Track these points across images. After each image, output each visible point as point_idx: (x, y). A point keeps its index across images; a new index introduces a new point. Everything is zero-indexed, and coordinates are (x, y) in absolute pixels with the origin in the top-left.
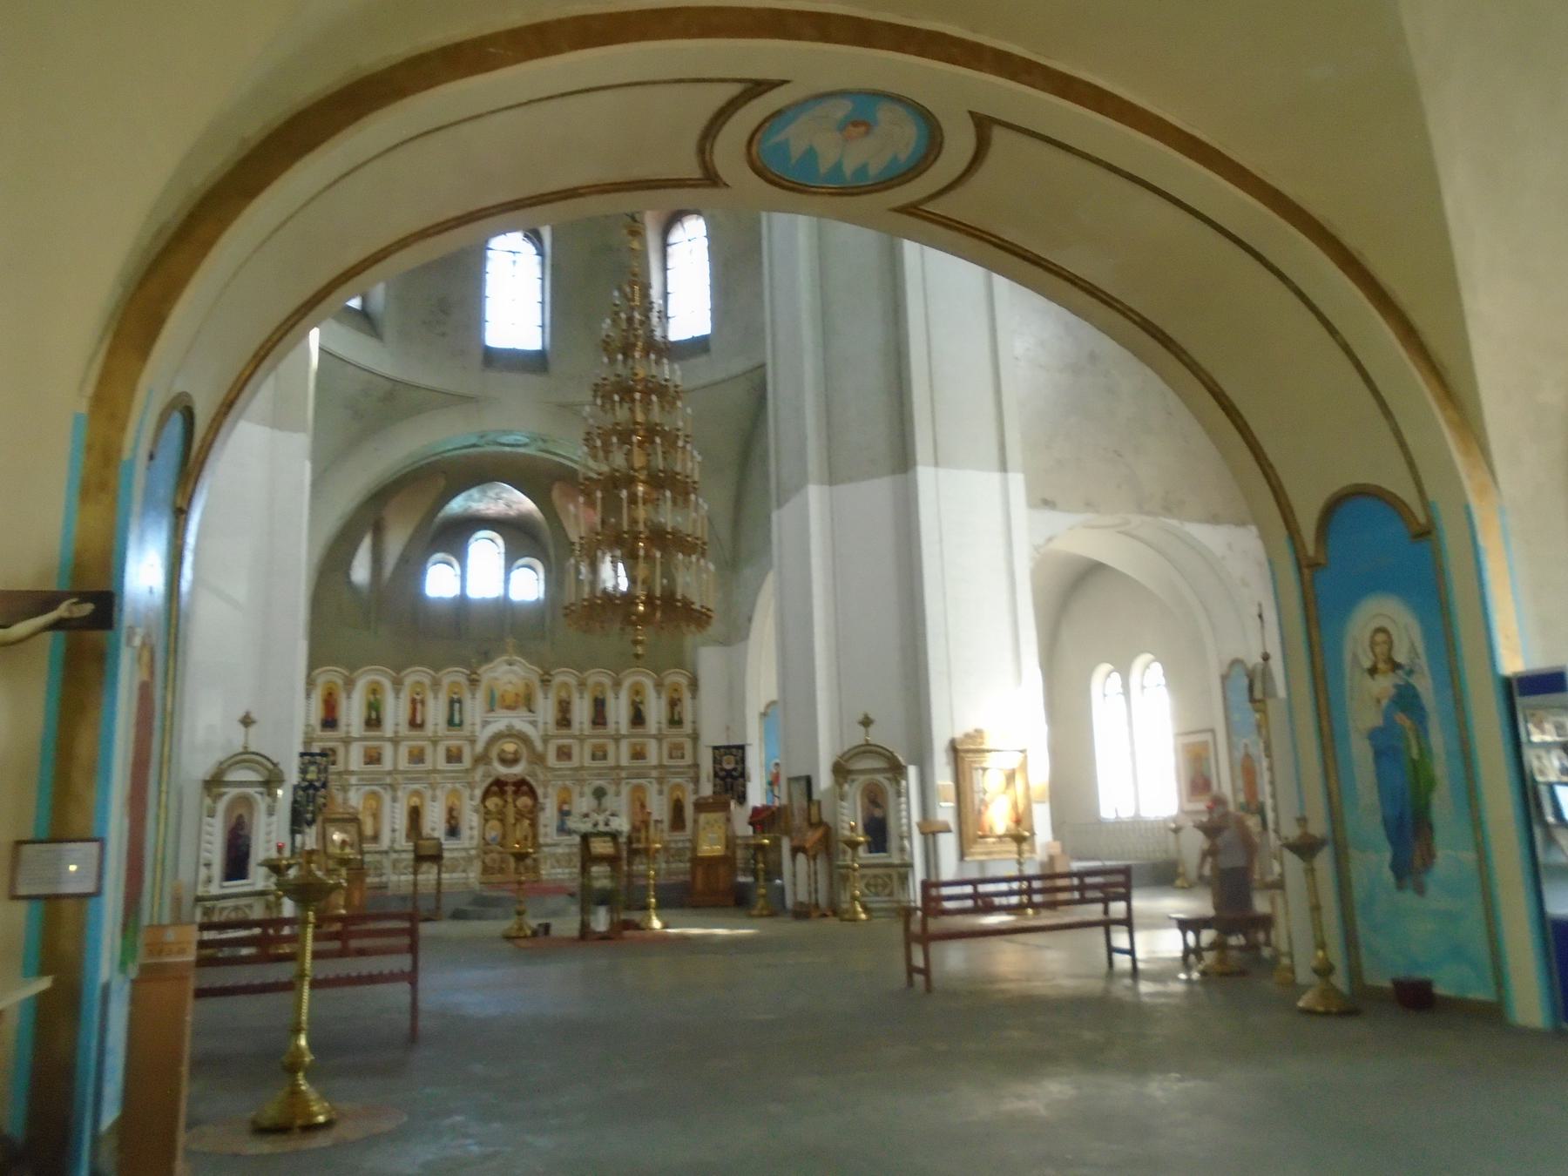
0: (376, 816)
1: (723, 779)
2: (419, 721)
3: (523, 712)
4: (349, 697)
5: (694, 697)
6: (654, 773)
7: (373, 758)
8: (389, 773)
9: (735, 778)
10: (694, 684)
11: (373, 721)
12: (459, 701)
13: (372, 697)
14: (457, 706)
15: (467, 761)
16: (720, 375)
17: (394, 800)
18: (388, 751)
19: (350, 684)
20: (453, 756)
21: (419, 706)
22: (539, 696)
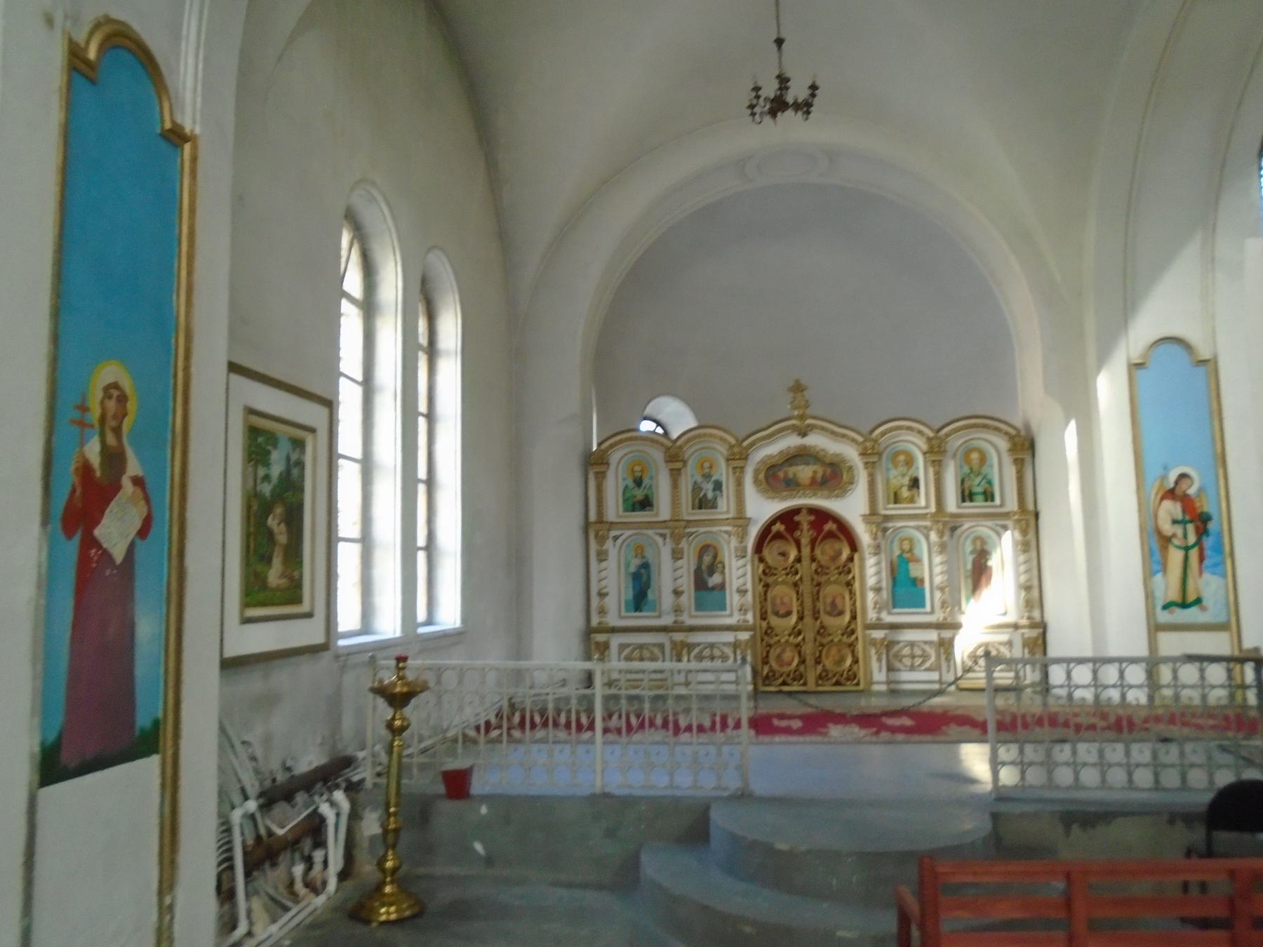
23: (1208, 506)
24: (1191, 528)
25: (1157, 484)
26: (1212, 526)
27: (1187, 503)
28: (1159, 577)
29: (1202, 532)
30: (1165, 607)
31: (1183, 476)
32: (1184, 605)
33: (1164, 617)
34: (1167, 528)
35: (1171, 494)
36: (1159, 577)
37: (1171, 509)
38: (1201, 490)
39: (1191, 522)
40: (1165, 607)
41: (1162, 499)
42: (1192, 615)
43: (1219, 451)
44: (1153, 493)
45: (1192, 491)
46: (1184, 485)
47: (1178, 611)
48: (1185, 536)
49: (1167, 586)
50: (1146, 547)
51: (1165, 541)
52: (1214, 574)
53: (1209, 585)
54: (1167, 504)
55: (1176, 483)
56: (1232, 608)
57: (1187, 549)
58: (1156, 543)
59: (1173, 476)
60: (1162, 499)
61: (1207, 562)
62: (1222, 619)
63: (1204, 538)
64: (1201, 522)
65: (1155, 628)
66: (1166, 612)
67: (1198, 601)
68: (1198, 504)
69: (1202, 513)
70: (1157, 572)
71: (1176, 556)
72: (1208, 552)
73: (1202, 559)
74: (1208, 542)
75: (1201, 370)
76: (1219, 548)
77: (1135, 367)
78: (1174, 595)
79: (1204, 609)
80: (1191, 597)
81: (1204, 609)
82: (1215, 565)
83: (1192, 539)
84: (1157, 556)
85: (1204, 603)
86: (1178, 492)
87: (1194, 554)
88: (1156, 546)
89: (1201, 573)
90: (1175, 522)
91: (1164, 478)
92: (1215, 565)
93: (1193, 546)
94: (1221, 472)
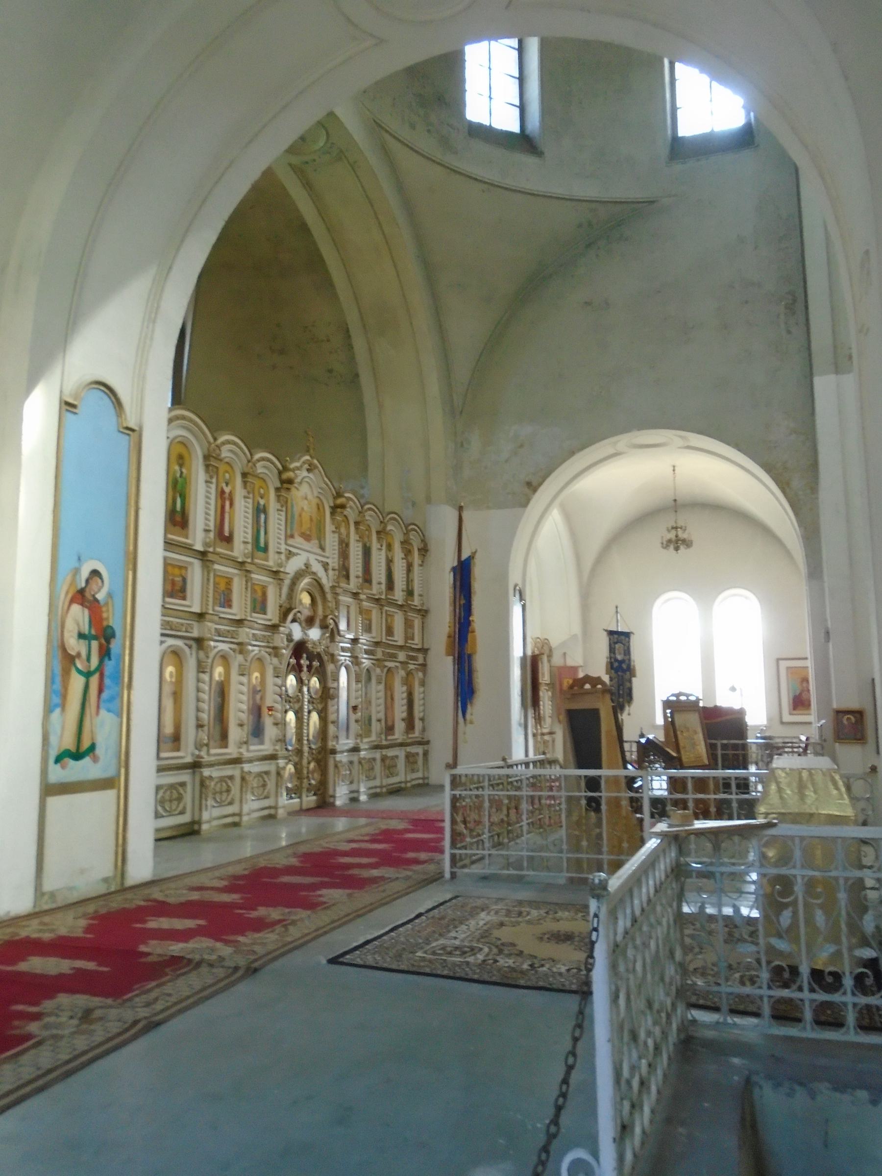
0: (177, 696)
1: (617, 670)
3: (313, 546)
6: (402, 656)
8: (201, 616)
9: (624, 671)
10: (424, 551)
12: (265, 510)
13: (177, 468)
14: (263, 516)
15: (272, 614)
16: (559, 191)
17: (201, 668)
18: (196, 574)
21: (227, 503)
22: (329, 527)
23: (114, 620)
24: (95, 644)
25: (69, 578)
26: (115, 646)
28: (58, 711)
29: (105, 653)
30: (58, 760)
31: (95, 573)
32: (77, 755)
33: (57, 774)
34: (74, 645)
35: (81, 596)
36: (58, 711)
38: (110, 595)
39: (96, 638)
41: (72, 601)
42: (83, 770)
43: (131, 548)
45: (100, 596)
46: (94, 586)
47: (71, 763)
48: (88, 659)
51: (69, 659)
52: (109, 711)
53: (103, 728)
54: (76, 608)
56: (123, 757)
58: (62, 660)
59: (85, 573)
60: (72, 601)
62: (110, 773)
63: (106, 659)
66: (58, 766)
67: (92, 748)
70: (56, 706)
71: (77, 682)
72: (107, 681)
73: (101, 691)
74: (109, 666)
76: (117, 677)
77: (68, 406)
78: (69, 743)
79: (95, 760)
80: (86, 744)
81: (95, 760)
82: (111, 699)
83: (95, 661)
84: (58, 686)
85: (99, 751)
86: (88, 595)
87: (94, 680)
88: (58, 669)
89: (97, 713)
90: (81, 636)
91: (77, 571)
92: (111, 699)
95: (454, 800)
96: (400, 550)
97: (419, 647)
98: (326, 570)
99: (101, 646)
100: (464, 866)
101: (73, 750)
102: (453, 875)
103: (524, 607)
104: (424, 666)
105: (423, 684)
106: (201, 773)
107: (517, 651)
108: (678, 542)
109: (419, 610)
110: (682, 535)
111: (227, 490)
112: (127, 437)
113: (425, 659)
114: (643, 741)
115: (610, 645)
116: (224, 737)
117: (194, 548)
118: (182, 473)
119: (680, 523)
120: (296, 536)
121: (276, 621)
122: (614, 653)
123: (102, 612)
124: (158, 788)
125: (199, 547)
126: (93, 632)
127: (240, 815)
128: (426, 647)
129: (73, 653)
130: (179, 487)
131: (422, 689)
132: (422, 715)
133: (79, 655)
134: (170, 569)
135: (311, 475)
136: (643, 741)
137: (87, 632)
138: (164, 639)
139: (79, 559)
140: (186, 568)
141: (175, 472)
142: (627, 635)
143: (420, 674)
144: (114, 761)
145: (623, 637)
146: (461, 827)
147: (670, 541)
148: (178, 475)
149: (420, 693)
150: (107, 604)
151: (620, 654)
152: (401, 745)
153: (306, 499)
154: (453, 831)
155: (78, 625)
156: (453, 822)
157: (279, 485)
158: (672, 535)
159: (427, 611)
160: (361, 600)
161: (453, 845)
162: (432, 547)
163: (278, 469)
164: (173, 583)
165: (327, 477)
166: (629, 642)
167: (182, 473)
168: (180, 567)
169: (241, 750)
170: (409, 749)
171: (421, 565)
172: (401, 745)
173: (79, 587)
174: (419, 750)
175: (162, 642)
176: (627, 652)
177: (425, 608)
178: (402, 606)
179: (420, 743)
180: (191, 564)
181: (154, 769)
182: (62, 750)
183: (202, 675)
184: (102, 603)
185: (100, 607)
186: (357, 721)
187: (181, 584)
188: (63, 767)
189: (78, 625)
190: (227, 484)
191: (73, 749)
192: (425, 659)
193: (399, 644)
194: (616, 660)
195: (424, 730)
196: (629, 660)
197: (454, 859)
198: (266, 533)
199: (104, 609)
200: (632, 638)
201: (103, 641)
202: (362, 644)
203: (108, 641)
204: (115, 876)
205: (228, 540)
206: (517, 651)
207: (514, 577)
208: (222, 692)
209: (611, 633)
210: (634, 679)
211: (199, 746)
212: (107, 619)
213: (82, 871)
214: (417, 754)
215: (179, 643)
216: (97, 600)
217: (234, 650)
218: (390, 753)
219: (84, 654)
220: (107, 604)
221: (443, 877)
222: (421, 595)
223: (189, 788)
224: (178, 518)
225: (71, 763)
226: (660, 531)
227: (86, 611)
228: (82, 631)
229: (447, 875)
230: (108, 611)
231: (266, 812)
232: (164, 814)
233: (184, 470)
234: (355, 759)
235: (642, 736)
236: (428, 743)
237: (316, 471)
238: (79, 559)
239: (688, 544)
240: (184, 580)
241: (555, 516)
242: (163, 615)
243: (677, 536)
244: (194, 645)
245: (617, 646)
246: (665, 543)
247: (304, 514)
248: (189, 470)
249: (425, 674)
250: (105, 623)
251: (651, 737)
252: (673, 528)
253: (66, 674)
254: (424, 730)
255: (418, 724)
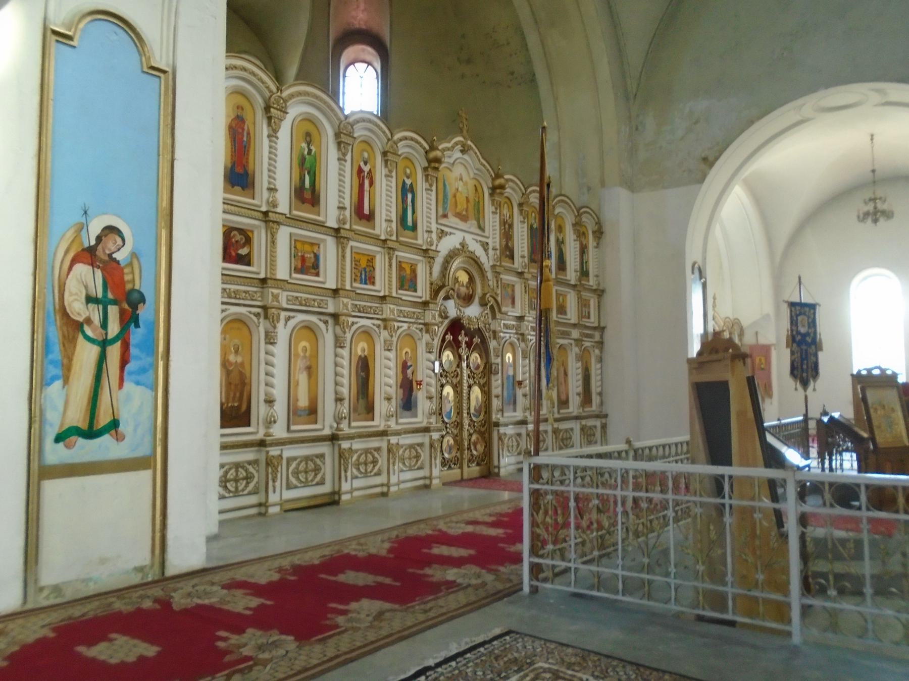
0: (311, 371)
1: (799, 344)
2: (366, 211)
3: (472, 225)
4: (273, 135)
5: (597, 247)
6: (575, 334)
7: (307, 264)
8: (335, 292)
9: (809, 345)
10: (599, 233)
11: (307, 195)
12: (412, 190)
13: (304, 145)
14: (410, 196)
15: (423, 291)
17: (339, 343)
18: (329, 250)
19: (272, 111)
20: (408, 281)
21: (367, 182)
22: (488, 208)
24: (113, 311)
25: (70, 235)
26: (144, 312)
27: (112, 271)
28: (58, 384)
29: (129, 319)
30: (58, 439)
31: (111, 230)
32: (91, 433)
33: (55, 454)
34: (78, 308)
35: (89, 255)
36: (58, 384)
37: (85, 278)
38: (134, 255)
39: (115, 302)
40: (58, 439)
42: (104, 448)
43: (165, 203)
44: (60, 248)
46: (110, 244)
47: (81, 441)
48: (104, 325)
49: (66, 403)
50: (39, 337)
51: (73, 328)
53: (131, 402)
54: (82, 269)
55: (99, 239)
57: (104, 344)
59: (95, 228)
61: (128, 367)
62: (144, 451)
64: (130, 304)
65: (39, 473)
66: (61, 444)
68: (127, 278)
69: (133, 290)
70: (54, 378)
71: (86, 354)
72: (133, 351)
74: (136, 335)
75: (152, 83)
76: (150, 346)
77: (55, 38)
78: (77, 416)
79: (119, 438)
80: (104, 419)
81: (119, 438)
82: (143, 370)
83: (114, 328)
84: (56, 353)
85: (121, 428)
86: (100, 252)
87: (114, 352)
88: (55, 335)
89: (121, 385)
90: (90, 299)
91: (81, 228)
92: (143, 370)
93: (114, 340)
94: (164, 233)
95: (536, 495)
96: (572, 232)
97: (596, 325)
98: (486, 250)
99: (122, 312)
100: (545, 580)
101: (84, 426)
102: (534, 590)
103: (704, 286)
104: (601, 344)
105: (600, 360)
106: (340, 446)
107: (697, 328)
108: (876, 214)
109: (595, 290)
110: (880, 206)
111: (366, 169)
112: (157, 80)
113: (602, 337)
114: (825, 419)
115: (791, 317)
116: (370, 410)
117: (328, 224)
118: (310, 151)
119: (879, 193)
120: (450, 215)
121: (426, 297)
122: (797, 325)
123: (123, 274)
124: (222, 466)
125: (332, 223)
126: (110, 296)
127: (388, 485)
128: (602, 325)
129: (81, 319)
130: (307, 165)
131: (599, 366)
132: (599, 390)
133: (88, 321)
134: (299, 245)
135: (466, 157)
136: (825, 419)
137: (100, 295)
138: (225, 307)
139: (86, 213)
140: (319, 245)
141: (302, 149)
142: (813, 307)
143: (597, 351)
144: (148, 438)
145: (807, 309)
146: (540, 531)
147: (867, 214)
148: (306, 152)
149: (596, 370)
150: (130, 264)
151: (803, 326)
152: (577, 418)
153: (461, 179)
154: (534, 537)
155: (86, 287)
156: (534, 524)
157: (427, 165)
158: (870, 207)
159: (603, 291)
160: (527, 279)
161: (534, 551)
162: (607, 228)
163: (424, 148)
164: (303, 259)
165: (483, 158)
166: (814, 314)
167: (310, 151)
168: (312, 244)
169: (389, 423)
170: (584, 422)
171: (597, 247)
172: (577, 418)
173: (86, 245)
174: (598, 423)
175: (223, 311)
176: (813, 324)
177: (601, 288)
178: (575, 286)
179: (597, 416)
180: (324, 241)
181: (217, 447)
182: (66, 427)
183: (339, 350)
184: (122, 264)
185: (122, 269)
186: (525, 395)
187: (313, 260)
188: (67, 447)
189: (86, 287)
190: (366, 163)
191: (84, 426)
192: (602, 337)
193: (573, 321)
194: (798, 333)
195: (602, 403)
196: (815, 333)
197: (536, 570)
198: (414, 212)
199: (126, 271)
200: (819, 310)
201: (126, 306)
202: (529, 321)
203: (135, 307)
204: (152, 566)
205: (369, 218)
206: (697, 328)
207: (693, 254)
208: (364, 367)
209: (792, 305)
210: (820, 354)
211: (338, 419)
212: (133, 281)
213: (103, 561)
214: (595, 427)
215: (314, 319)
216: (118, 262)
217: (378, 326)
218: (590, 423)
219: (96, 319)
220: (130, 264)
221: (521, 589)
222: (597, 276)
223: (328, 460)
224: (308, 195)
225: (75, 442)
226: (860, 205)
227: (99, 273)
228: (93, 294)
229: (526, 589)
230: (133, 273)
231: (421, 482)
232: (227, 495)
233: (312, 148)
234: (523, 431)
235: (825, 413)
236: (606, 416)
237: (471, 152)
238: (86, 213)
239: (888, 215)
240: (317, 257)
241: (738, 196)
242: (223, 283)
243: (875, 208)
244: (331, 321)
245: (800, 318)
246: (862, 216)
247: (458, 195)
248: (319, 147)
249: (601, 352)
250: (129, 287)
251: (836, 415)
252: (870, 200)
253: (69, 342)
254: (602, 403)
255: (596, 399)
